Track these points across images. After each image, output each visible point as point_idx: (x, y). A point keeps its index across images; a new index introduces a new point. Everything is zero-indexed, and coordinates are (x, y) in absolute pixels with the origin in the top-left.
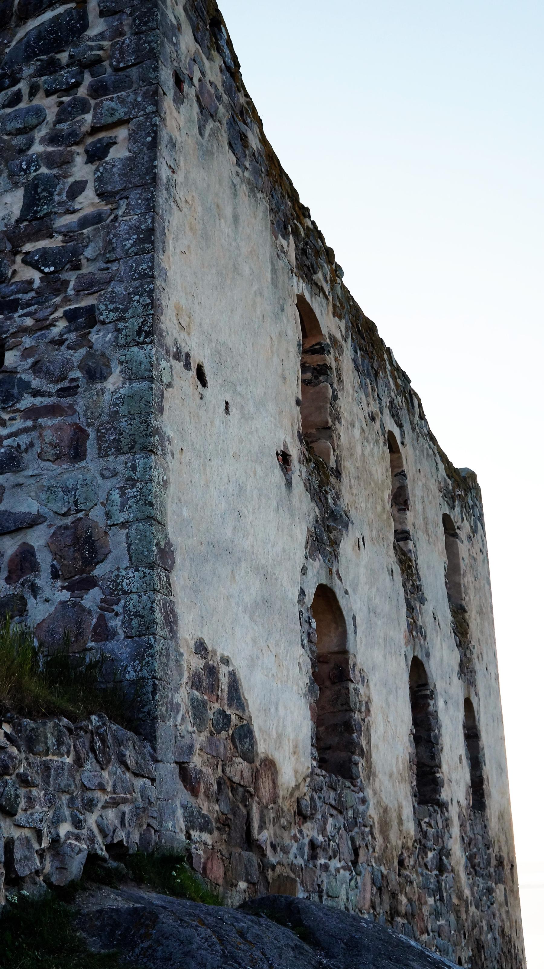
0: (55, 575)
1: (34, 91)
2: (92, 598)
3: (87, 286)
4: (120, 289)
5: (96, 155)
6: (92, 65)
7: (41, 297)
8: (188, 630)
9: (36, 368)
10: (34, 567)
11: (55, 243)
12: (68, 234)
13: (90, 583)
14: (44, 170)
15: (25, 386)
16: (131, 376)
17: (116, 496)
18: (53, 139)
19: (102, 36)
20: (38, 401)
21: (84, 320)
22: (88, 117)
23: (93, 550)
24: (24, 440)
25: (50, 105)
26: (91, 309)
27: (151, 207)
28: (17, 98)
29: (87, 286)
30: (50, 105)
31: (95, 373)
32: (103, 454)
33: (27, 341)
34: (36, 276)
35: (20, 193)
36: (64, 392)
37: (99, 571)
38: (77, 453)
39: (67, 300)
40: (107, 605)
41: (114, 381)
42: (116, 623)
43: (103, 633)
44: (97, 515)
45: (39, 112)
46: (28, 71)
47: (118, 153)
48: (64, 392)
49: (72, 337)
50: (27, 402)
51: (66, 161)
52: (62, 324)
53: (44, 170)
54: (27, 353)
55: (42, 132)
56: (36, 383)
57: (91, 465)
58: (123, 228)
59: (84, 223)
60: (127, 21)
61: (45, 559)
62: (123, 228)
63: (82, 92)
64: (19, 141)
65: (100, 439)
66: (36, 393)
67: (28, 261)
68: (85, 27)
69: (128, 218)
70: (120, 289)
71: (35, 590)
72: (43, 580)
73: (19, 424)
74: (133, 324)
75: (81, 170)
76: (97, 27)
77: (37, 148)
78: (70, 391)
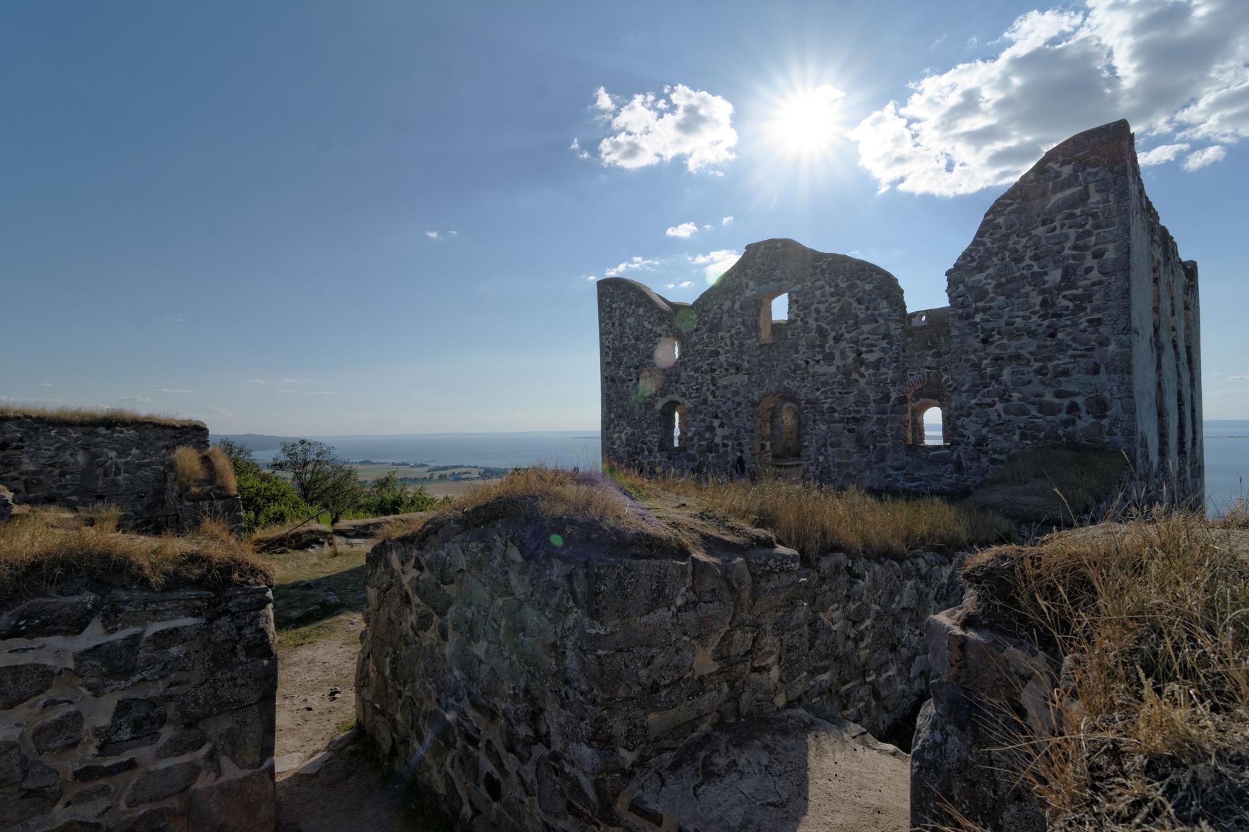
0: (1088, 413)
1: (1063, 226)
2: (1105, 422)
3: (1097, 309)
4: (1114, 312)
5: (1098, 255)
6: (1094, 216)
7: (1074, 313)
8: (1140, 429)
9: (1074, 340)
10: (1079, 410)
11: (1080, 291)
12: (1086, 288)
13: (1105, 417)
14: (1071, 261)
15: (1070, 346)
16: (1120, 344)
17: (1115, 388)
18: (1075, 248)
19: (1098, 202)
20: (1076, 352)
22: (1093, 239)
23: (1105, 405)
24: (1070, 366)
25: (1072, 233)
26: (1099, 319)
27: (1128, 279)
28: (1054, 229)
29: (1097, 309)
30: (1072, 233)
31: (1103, 343)
32: (1108, 373)
33: (1069, 330)
34: (1071, 305)
35: (1060, 271)
36: (1087, 350)
37: (1108, 413)
38: (1095, 371)
39: (1087, 315)
40: (1112, 425)
41: (1112, 347)
42: (1116, 430)
43: (1111, 433)
44: (1107, 394)
45: (1067, 236)
46: (1059, 217)
47: (1110, 255)
48: (1087, 350)
49: (1091, 330)
50: (1070, 352)
51: (1083, 258)
52: (1085, 324)
53: (1071, 261)
54: (1068, 334)
55: (1069, 244)
56: (1074, 346)
57: (1103, 376)
58: (1114, 288)
59: (1094, 284)
60: (1111, 196)
61: (1083, 408)
62: (1114, 288)
63: (1088, 227)
64: (1057, 248)
65: (1107, 368)
66: (1075, 349)
67: (1064, 297)
68: (1088, 198)
69: (1116, 283)
70: (1114, 312)
71: (1080, 418)
72: (1083, 414)
73: (1067, 360)
74: (1120, 326)
75: (1090, 262)
76: (1095, 198)
77: (1067, 252)
78: (1092, 349)
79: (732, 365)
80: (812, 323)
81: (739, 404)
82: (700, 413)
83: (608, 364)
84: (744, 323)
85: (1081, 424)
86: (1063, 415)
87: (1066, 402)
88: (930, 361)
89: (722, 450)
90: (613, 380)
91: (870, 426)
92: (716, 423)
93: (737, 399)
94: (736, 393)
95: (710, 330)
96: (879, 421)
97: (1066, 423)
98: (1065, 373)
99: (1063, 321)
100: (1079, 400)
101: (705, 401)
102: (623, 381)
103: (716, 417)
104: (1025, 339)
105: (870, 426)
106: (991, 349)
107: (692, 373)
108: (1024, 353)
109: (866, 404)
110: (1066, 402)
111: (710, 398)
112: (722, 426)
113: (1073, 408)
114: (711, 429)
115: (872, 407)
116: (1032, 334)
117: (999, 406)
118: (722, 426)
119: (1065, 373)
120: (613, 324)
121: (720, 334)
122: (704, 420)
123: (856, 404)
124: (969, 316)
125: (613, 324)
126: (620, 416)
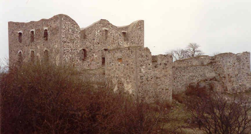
21: (142, 43)
79: (97, 42)
81: (99, 51)
83: (63, 37)
89: (95, 60)
90: (65, 42)
92: (94, 54)
102: (68, 43)
103: (94, 53)
107: (89, 43)
114: (93, 55)
122: (91, 54)
125: (66, 27)
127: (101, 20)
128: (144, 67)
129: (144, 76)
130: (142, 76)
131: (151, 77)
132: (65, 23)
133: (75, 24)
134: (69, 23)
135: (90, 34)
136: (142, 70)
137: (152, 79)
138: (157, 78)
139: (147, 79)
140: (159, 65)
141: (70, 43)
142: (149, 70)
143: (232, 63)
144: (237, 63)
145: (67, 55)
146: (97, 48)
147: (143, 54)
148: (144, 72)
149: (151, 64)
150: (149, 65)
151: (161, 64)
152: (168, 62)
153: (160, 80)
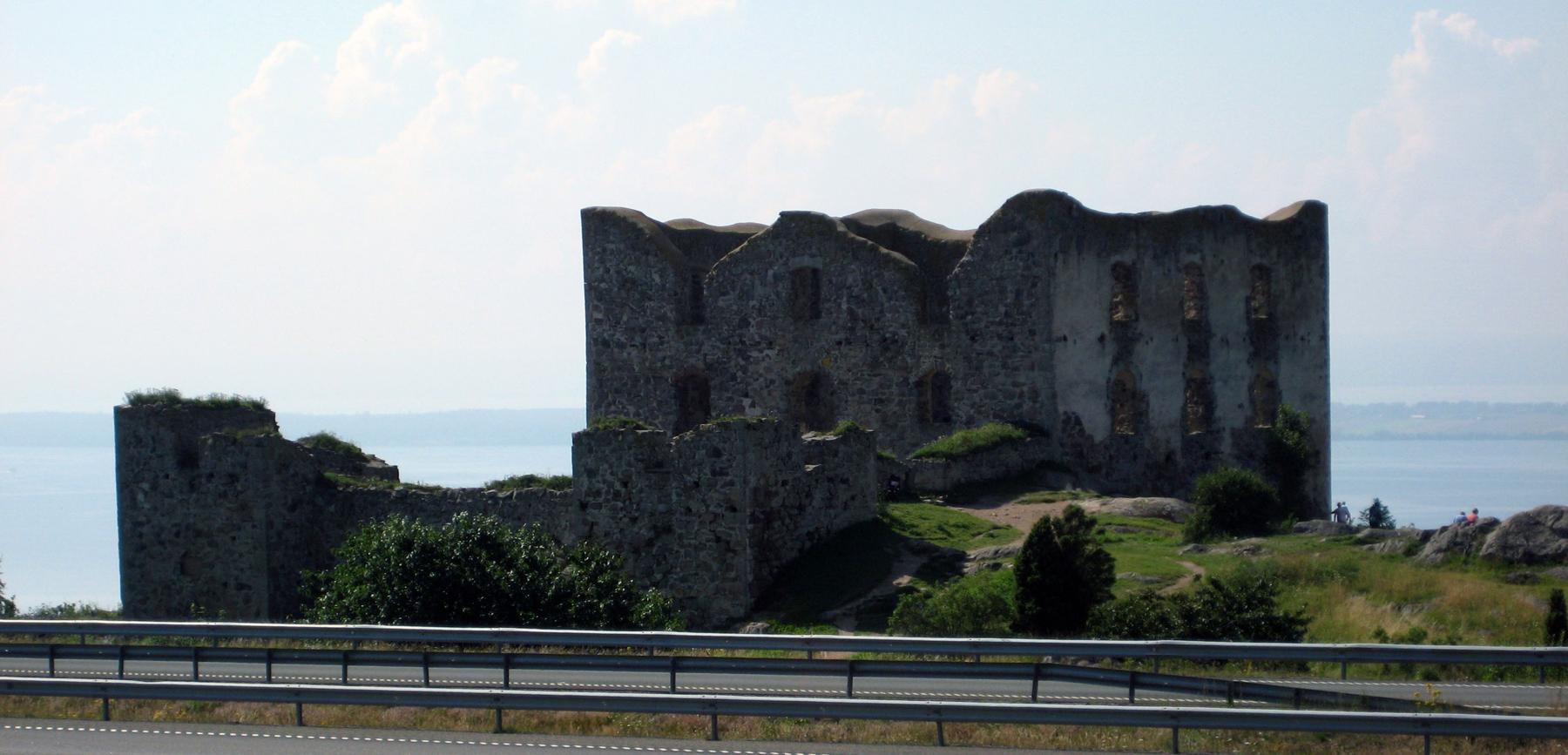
21: (1032, 333)
80: (844, 307)
81: (772, 382)
82: (727, 390)
83: (599, 322)
84: (778, 294)
85: (1025, 407)
86: (1016, 401)
87: (1018, 390)
88: (936, 352)
90: (606, 344)
91: (893, 407)
92: (747, 402)
93: (772, 376)
94: (768, 370)
95: (740, 298)
96: (900, 403)
97: (1019, 406)
98: (1016, 369)
99: (1016, 330)
100: (1025, 389)
101: (734, 378)
102: (622, 346)
103: (746, 395)
104: (996, 340)
105: (893, 407)
106: (977, 346)
108: (995, 350)
109: (890, 387)
110: (1018, 390)
111: (740, 374)
112: (753, 405)
113: (1021, 395)
114: (741, 409)
115: (894, 389)
116: (1000, 337)
117: (982, 392)
118: (753, 405)
119: (1016, 369)
120: (608, 271)
121: (752, 303)
122: (730, 399)
123: (881, 386)
124: (963, 317)
125: (608, 271)
126: (617, 391)
127: (782, 214)
128: (146, 486)
129: (149, 522)
130: (141, 524)
131: (174, 530)
132: (604, 250)
133: (647, 253)
134: (622, 246)
135: (724, 294)
136: (141, 497)
137: (177, 534)
138: (199, 534)
139: (158, 535)
140: (203, 480)
141: (630, 349)
142: (167, 501)
143: (609, 478)
144: (639, 483)
145: (613, 408)
146: (761, 368)
147: (142, 431)
148: (147, 506)
149: (172, 475)
150: (167, 476)
151: (211, 475)
152: (244, 466)
153: (210, 544)
